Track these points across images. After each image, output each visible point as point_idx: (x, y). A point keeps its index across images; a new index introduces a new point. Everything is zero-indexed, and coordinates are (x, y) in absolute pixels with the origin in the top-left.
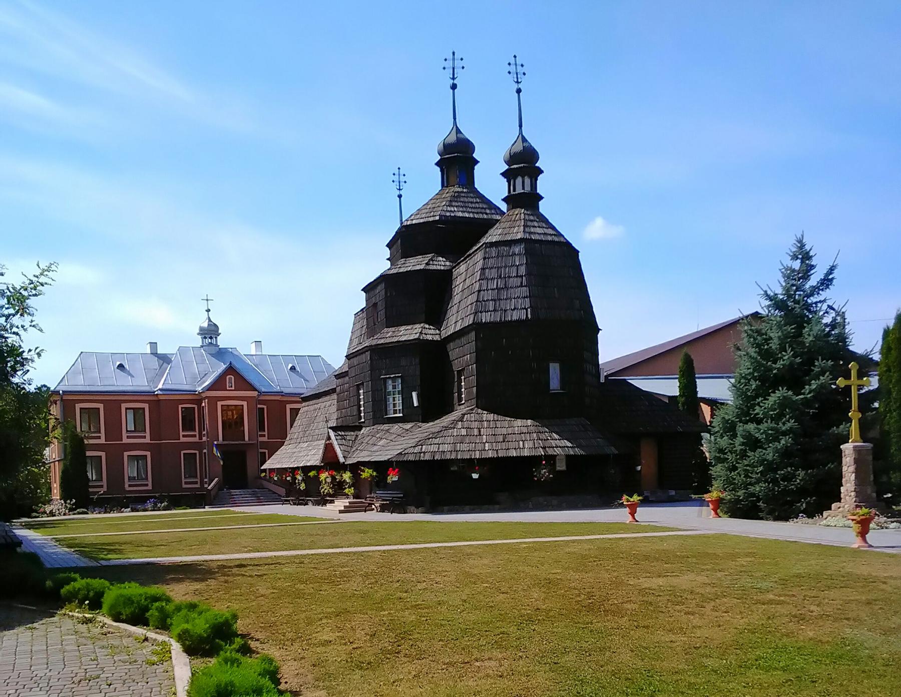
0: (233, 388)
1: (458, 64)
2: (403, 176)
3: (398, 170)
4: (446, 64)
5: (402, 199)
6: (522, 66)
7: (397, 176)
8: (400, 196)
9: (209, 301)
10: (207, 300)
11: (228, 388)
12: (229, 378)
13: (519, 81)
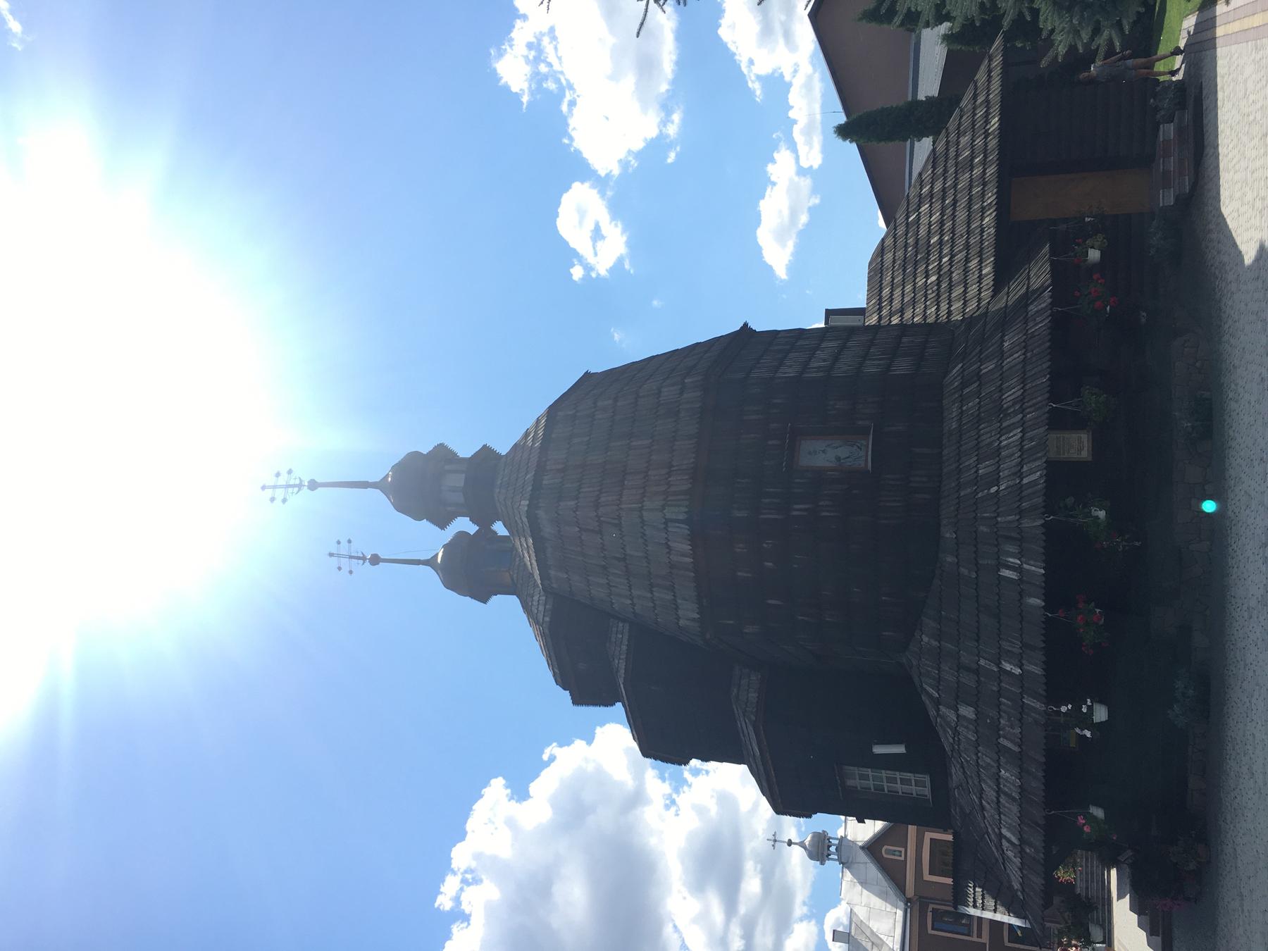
0: (903, 850)
1: (344, 549)
4: (346, 569)
6: (278, 475)
10: (775, 841)
11: (902, 858)
12: (886, 853)
13: (297, 482)
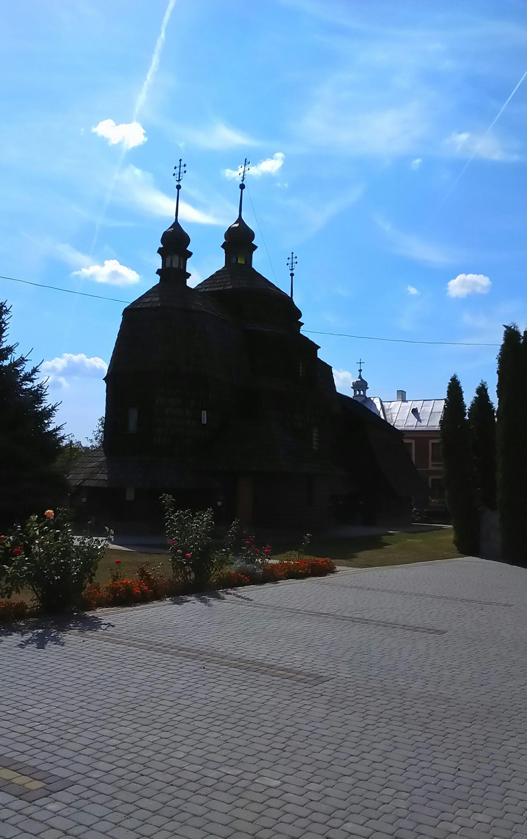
2: (295, 259)
3: (291, 254)
5: (293, 277)
7: (290, 260)
8: (292, 275)
9: (359, 364)
10: (360, 363)
